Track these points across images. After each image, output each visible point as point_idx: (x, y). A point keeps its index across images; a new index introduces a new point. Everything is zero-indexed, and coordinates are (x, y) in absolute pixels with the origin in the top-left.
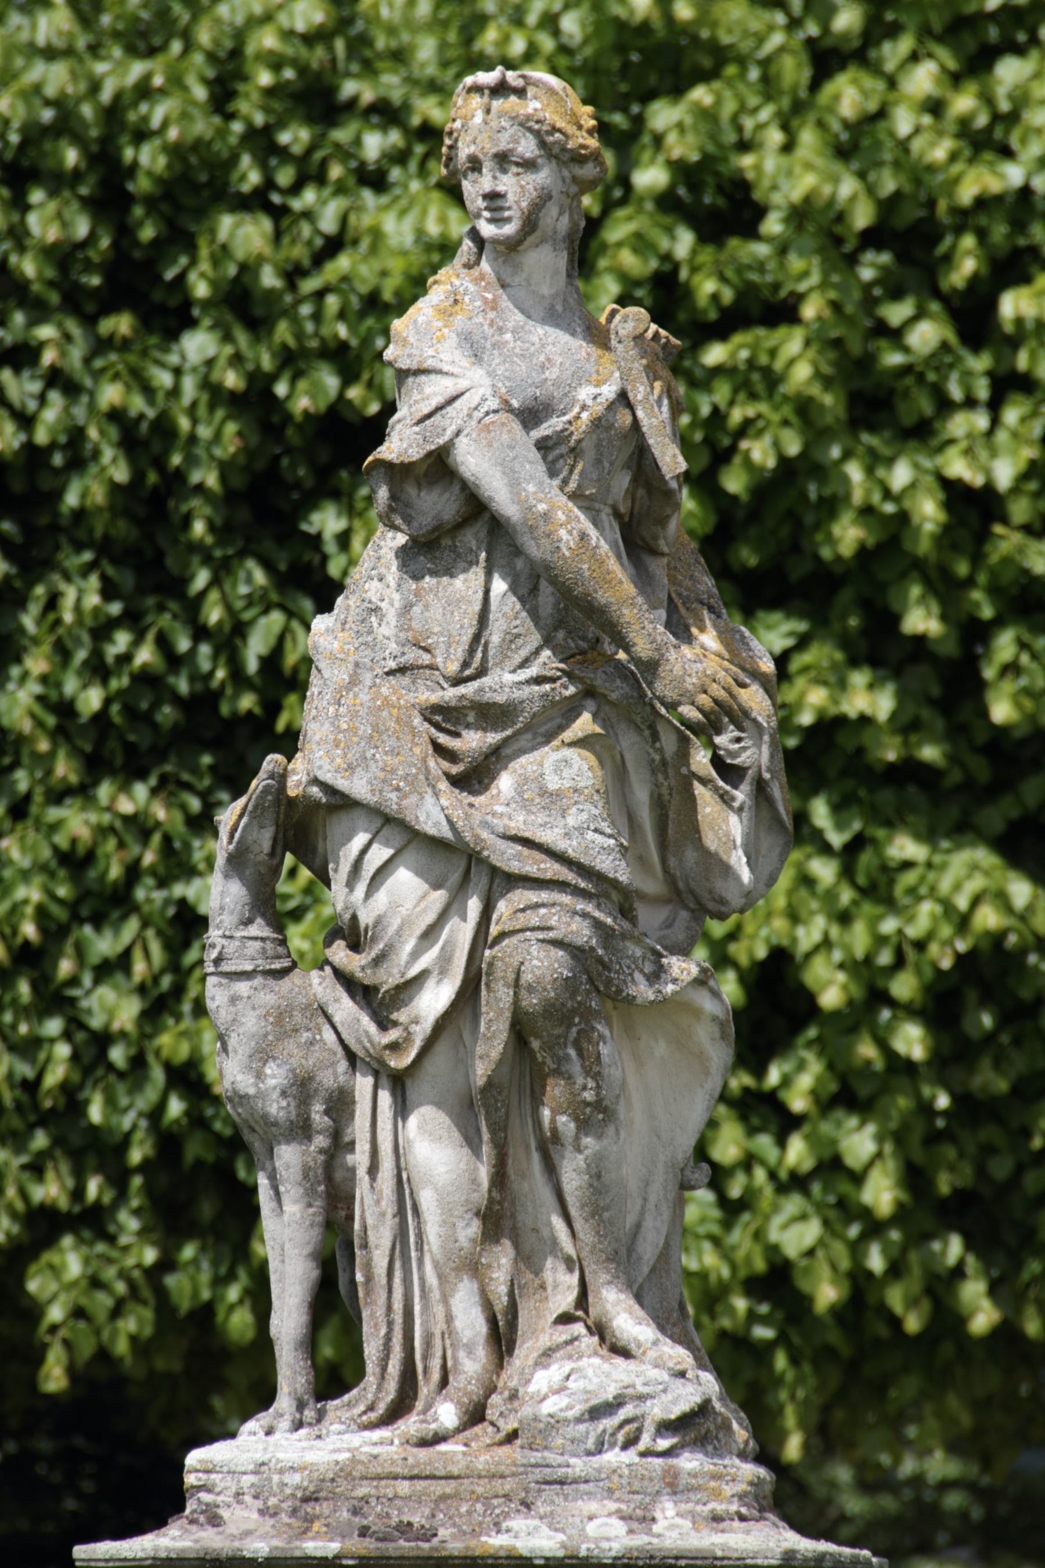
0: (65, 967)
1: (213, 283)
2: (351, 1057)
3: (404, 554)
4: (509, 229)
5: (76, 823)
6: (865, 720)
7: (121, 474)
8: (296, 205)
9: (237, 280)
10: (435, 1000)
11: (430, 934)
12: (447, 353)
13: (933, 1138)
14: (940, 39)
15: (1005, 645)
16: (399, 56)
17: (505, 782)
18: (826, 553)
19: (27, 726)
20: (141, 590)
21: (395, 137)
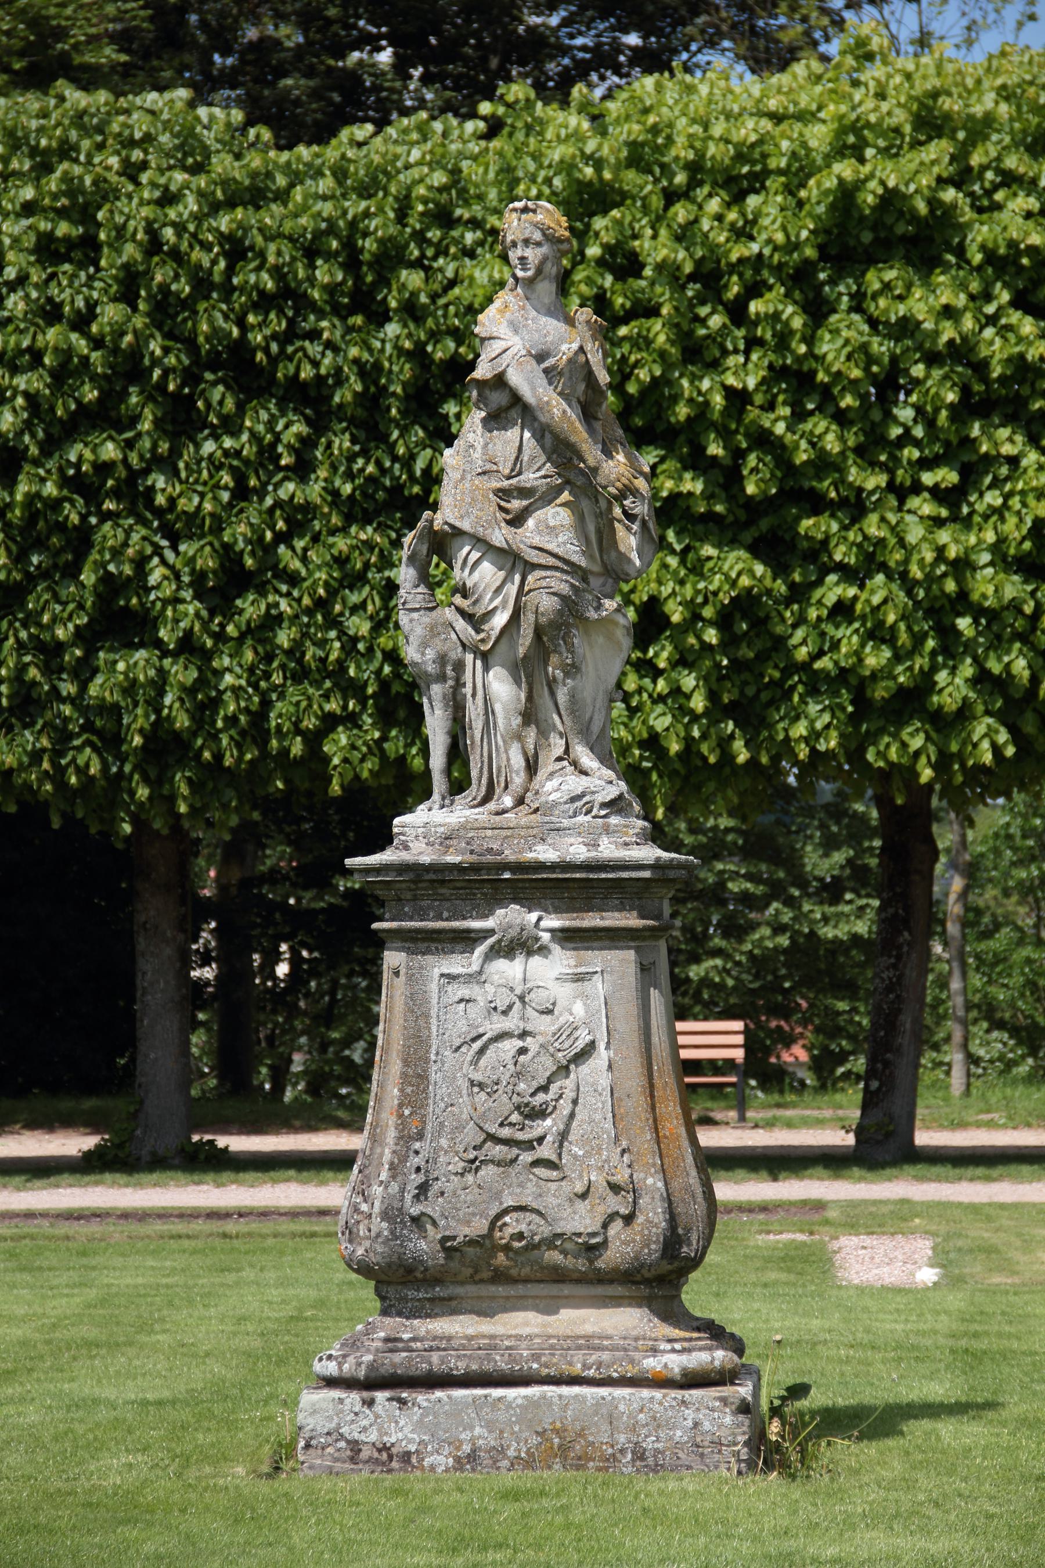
0: (338, 608)
1: (398, 301)
2: (463, 645)
3: (485, 421)
4: (530, 273)
5: (341, 544)
6: (690, 494)
7: (359, 388)
8: (435, 265)
9: (409, 299)
10: (500, 620)
11: (498, 590)
12: (502, 330)
13: (721, 678)
14: (721, 187)
15: (752, 460)
16: (481, 197)
17: (531, 523)
18: (673, 419)
19: (319, 501)
20: (368, 440)
21: (479, 234)
